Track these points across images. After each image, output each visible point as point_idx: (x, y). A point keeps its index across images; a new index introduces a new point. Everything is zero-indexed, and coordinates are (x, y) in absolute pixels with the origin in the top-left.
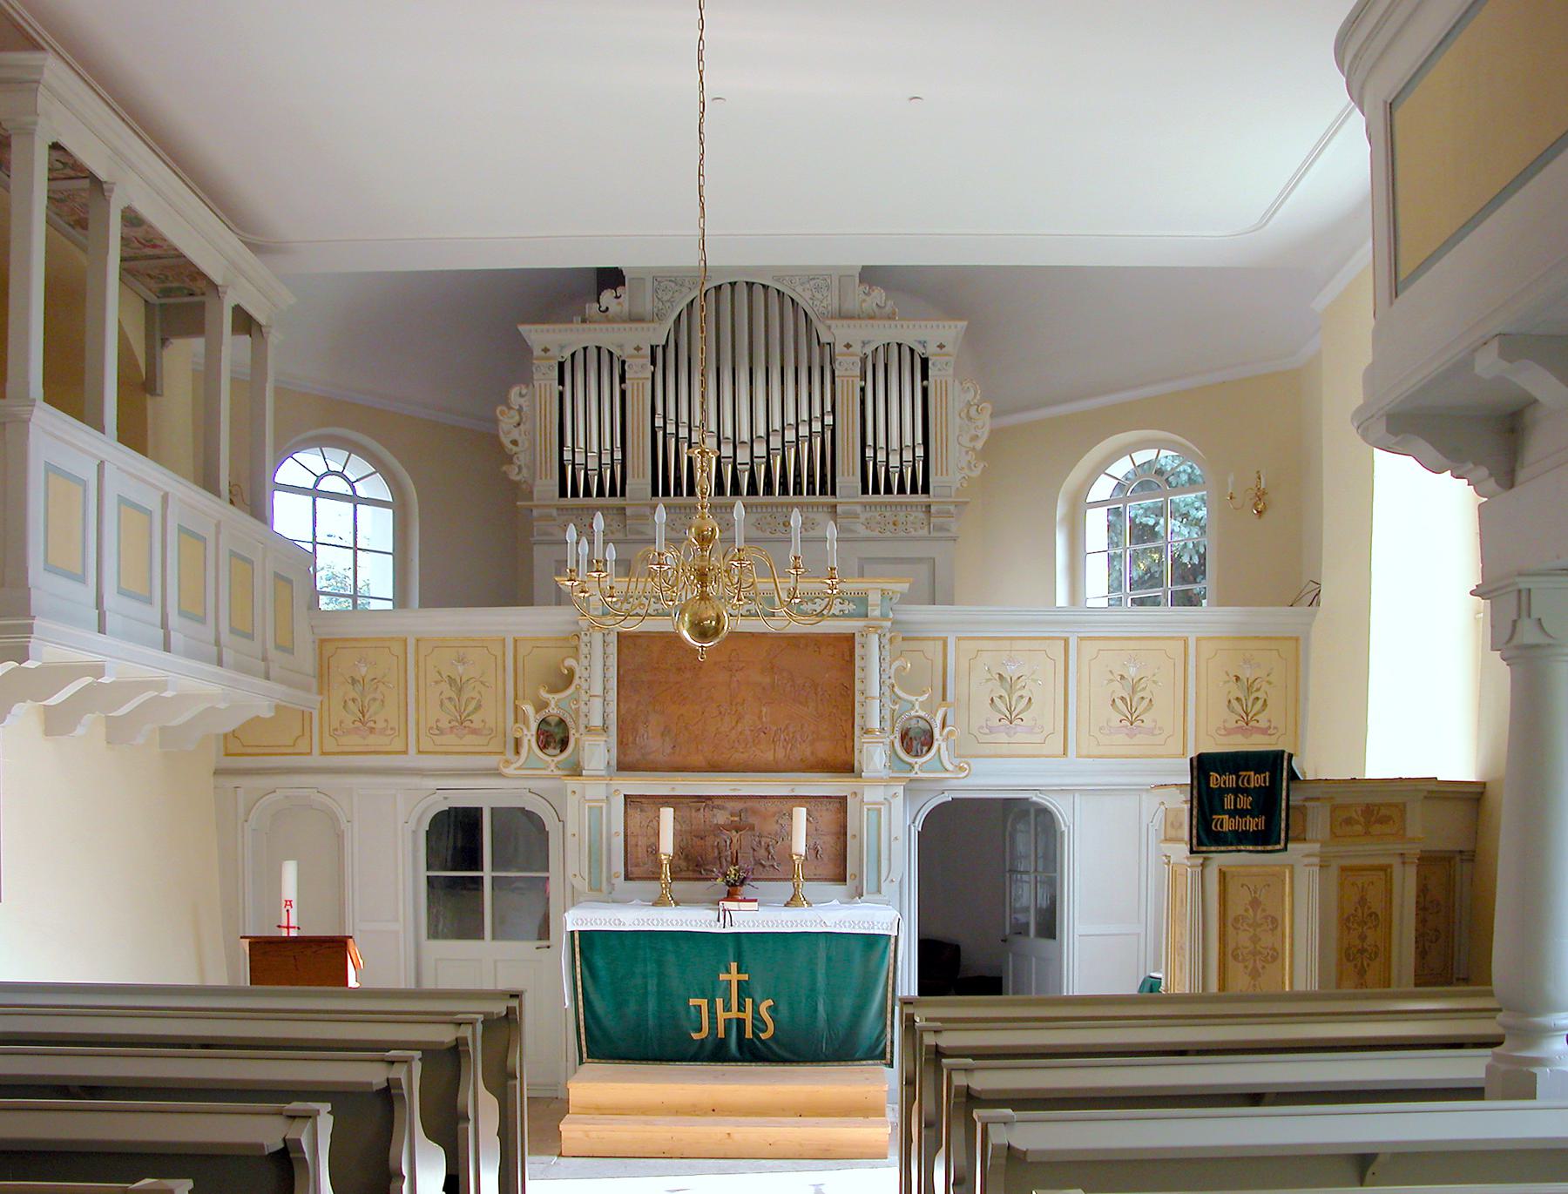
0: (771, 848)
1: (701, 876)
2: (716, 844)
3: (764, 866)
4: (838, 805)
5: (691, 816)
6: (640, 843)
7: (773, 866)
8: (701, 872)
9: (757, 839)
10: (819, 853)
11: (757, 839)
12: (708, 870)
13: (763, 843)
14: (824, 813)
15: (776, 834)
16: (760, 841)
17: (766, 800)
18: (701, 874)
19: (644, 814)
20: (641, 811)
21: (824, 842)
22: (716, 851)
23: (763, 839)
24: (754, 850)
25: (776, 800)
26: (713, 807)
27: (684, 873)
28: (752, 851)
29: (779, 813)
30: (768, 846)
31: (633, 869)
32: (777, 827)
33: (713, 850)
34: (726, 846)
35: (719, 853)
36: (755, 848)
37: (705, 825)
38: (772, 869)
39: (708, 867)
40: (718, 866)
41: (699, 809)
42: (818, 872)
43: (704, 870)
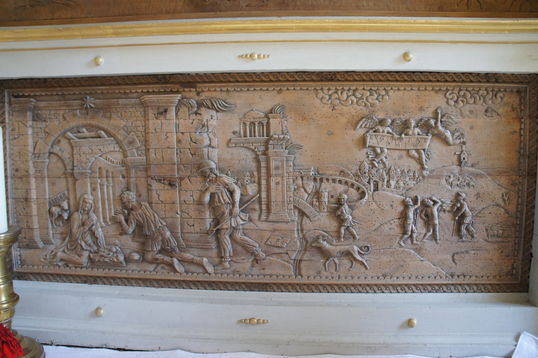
0: (346, 208)
1: (172, 276)
2: (207, 198)
3: (326, 255)
4: (514, 99)
5: (146, 127)
6: (34, 195)
7: (348, 254)
8: (171, 265)
9: (311, 186)
10: (467, 220)
11: (311, 186)
12: (191, 262)
13: (325, 198)
14: (481, 120)
15: (360, 173)
16: (318, 194)
17: (333, 85)
18: (175, 271)
19: (42, 125)
20: (36, 118)
21: (478, 195)
22: (208, 215)
23: (325, 185)
24: (302, 214)
25: (360, 86)
26: (200, 105)
27: (133, 266)
28: (295, 216)
29: (367, 117)
30: (339, 203)
31: (24, 252)
32: (361, 155)
33: (200, 212)
34: (233, 204)
35: (217, 221)
36: (309, 209)
37: (180, 151)
38: (346, 262)
39: (188, 256)
40: (214, 252)
41: (166, 111)
42: (458, 269)
43: (182, 261)
